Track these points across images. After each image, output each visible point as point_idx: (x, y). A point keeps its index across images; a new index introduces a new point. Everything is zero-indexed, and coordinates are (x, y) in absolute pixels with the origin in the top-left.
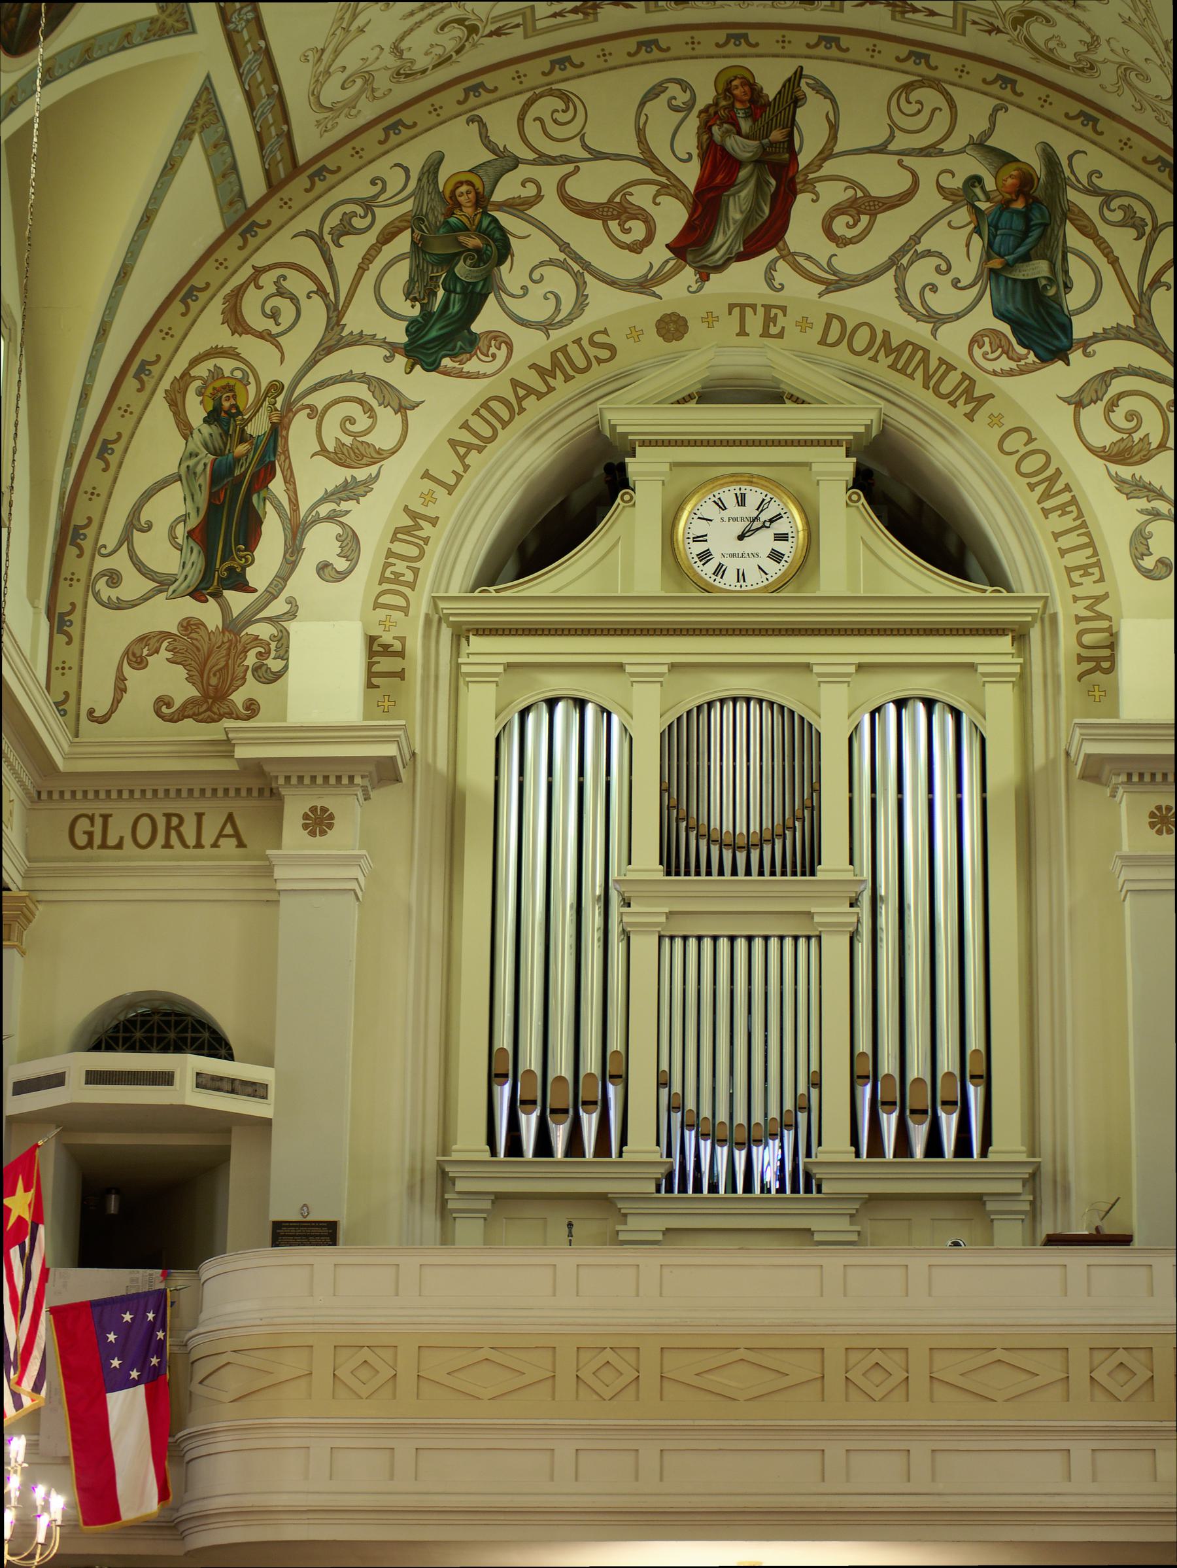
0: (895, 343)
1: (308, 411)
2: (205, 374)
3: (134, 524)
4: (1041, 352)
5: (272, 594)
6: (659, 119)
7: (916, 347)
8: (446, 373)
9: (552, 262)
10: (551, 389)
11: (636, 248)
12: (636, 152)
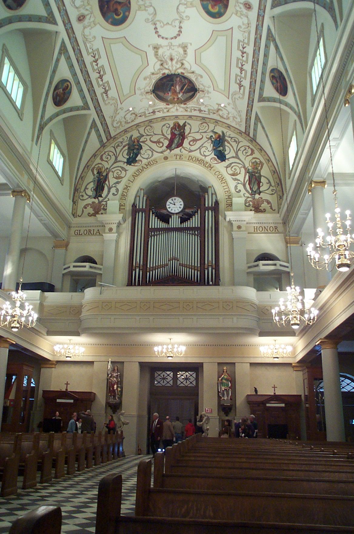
0: (199, 159)
3: (86, 188)
5: (106, 198)
6: (165, 129)
7: (202, 160)
8: (132, 166)
9: (148, 150)
10: (147, 167)
11: (161, 147)
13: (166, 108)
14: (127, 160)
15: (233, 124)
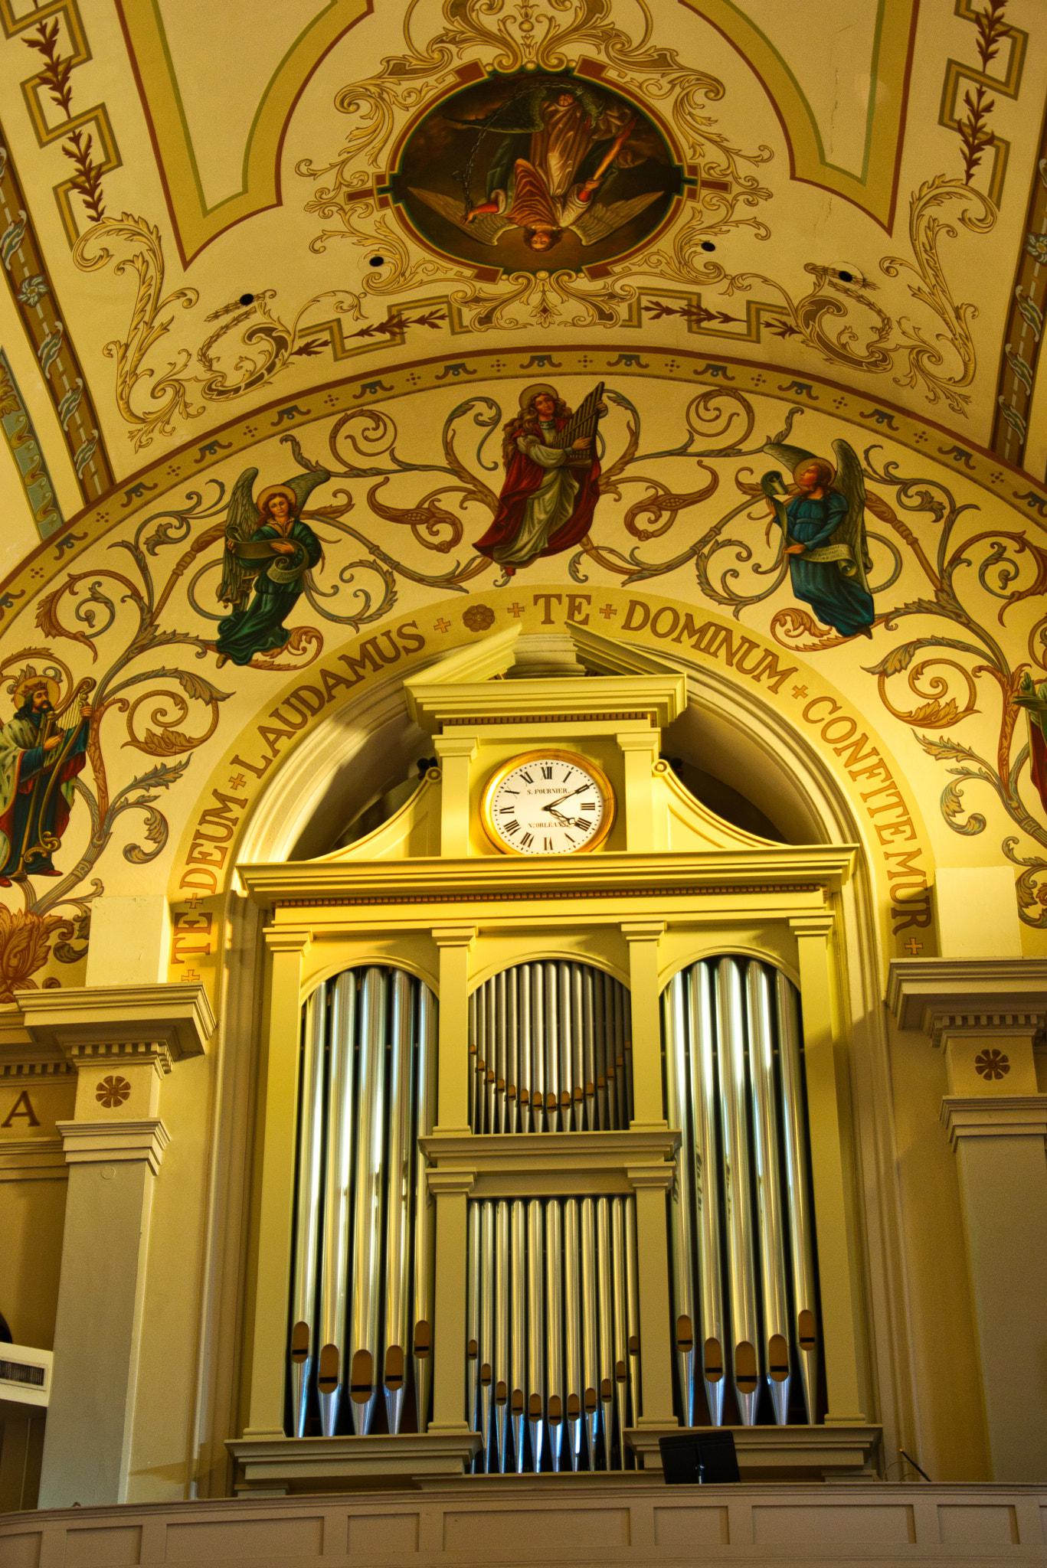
0: (698, 624)
1: (120, 705)
2: (18, 673)
4: (843, 628)
5: (77, 877)
7: (719, 628)
9: (361, 563)
10: (360, 678)
11: (444, 548)
12: (444, 463)
13: (477, 300)
14: (220, 630)
15: (915, 397)
